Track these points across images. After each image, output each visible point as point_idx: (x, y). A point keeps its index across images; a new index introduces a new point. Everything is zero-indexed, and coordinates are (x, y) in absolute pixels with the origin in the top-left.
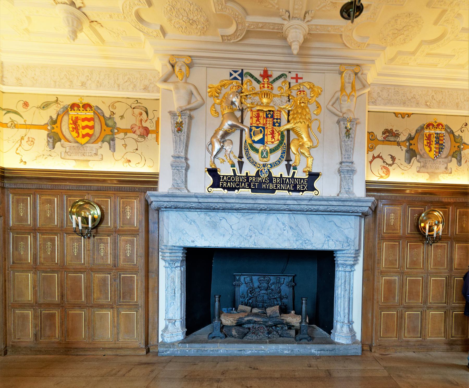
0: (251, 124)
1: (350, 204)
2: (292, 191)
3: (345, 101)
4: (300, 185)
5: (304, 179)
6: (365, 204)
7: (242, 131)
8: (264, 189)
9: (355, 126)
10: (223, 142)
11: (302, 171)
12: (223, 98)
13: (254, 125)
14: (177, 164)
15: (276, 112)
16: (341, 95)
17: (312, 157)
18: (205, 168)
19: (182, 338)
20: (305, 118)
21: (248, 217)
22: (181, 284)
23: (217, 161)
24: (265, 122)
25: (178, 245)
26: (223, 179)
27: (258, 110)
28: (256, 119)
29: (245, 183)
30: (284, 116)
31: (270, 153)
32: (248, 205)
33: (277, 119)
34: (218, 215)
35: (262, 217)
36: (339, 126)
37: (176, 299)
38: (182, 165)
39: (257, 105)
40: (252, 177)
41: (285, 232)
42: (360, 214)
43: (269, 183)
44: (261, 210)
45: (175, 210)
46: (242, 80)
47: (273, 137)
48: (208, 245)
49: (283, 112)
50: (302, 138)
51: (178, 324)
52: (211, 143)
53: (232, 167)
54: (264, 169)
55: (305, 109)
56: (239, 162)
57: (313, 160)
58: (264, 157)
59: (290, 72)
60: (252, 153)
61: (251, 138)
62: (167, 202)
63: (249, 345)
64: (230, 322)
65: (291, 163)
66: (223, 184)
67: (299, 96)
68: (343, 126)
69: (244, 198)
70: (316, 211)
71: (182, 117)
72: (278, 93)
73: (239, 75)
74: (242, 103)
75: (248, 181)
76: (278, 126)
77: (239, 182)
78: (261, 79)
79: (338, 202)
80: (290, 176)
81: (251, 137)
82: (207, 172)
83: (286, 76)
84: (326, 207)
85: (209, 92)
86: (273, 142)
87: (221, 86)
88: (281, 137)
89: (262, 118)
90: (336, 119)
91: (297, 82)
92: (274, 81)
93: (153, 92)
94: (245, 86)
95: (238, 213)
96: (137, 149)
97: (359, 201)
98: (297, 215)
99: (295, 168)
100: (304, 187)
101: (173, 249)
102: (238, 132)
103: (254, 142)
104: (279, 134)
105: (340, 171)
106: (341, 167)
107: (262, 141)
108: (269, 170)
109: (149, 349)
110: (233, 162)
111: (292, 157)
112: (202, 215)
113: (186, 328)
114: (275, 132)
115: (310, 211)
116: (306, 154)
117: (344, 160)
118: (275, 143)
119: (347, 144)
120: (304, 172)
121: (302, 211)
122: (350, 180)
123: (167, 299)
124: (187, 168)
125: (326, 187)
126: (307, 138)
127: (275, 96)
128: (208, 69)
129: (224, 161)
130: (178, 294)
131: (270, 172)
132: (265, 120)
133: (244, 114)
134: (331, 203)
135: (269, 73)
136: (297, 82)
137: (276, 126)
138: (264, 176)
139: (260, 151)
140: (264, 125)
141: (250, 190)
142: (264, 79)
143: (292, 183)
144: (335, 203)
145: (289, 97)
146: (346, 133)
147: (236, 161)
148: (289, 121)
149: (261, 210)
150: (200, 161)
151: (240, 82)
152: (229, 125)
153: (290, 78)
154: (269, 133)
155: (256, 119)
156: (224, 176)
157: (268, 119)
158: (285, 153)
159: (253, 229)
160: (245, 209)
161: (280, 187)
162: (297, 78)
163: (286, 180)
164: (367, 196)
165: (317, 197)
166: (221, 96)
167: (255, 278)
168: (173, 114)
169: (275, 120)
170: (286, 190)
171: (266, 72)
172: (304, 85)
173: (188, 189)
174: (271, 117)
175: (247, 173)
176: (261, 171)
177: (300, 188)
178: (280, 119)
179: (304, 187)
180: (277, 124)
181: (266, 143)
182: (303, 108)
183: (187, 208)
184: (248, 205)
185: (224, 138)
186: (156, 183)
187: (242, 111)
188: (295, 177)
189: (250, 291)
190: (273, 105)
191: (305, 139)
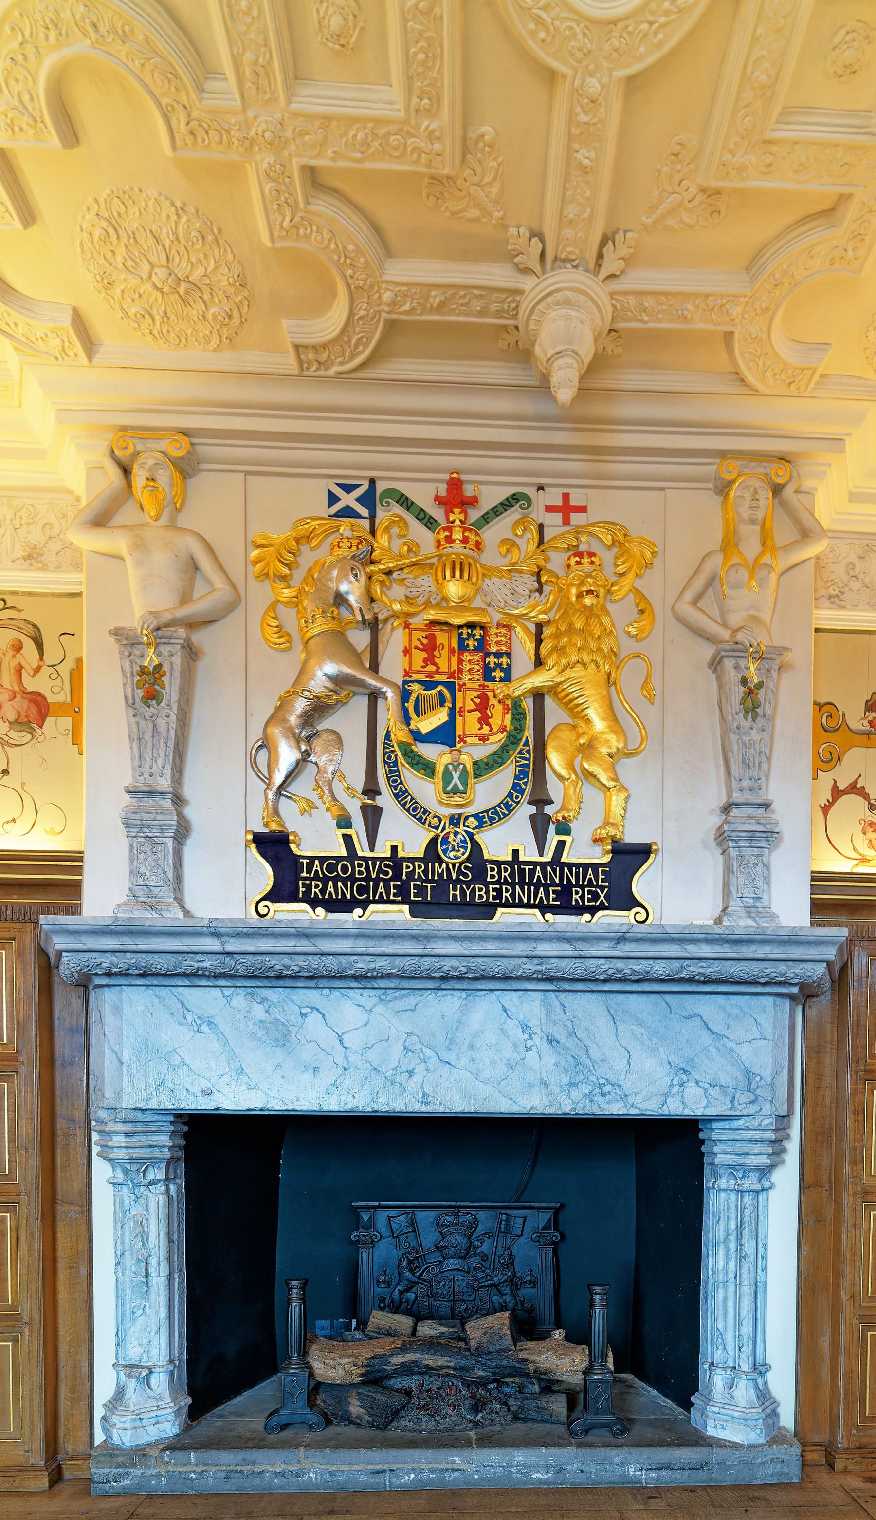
0: (407, 674)
2: (555, 910)
3: (738, 586)
4: (583, 887)
5: (595, 867)
6: (812, 953)
7: (375, 697)
8: (455, 904)
9: (774, 674)
10: (309, 739)
12: (305, 581)
13: (415, 677)
14: (146, 816)
15: (493, 631)
16: (724, 564)
17: (623, 788)
18: (247, 832)
19: (176, 1430)
20: (599, 649)
21: (399, 1005)
22: (170, 1241)
23: (285, 805)
24: (454, 667)
25: (154, 1104)
27: (433, 623)
28: (424, 655)
29: (386, 883)
30: (523, 646)
31: (476, 776)
32: (399, 962)
33: (498, 655)
34: (295, 998)
35: (450, 1003)
36: (719, 678)
37: (153, 1296)
38: (162, 821)
39: (428, 604)
40: (412, 860)
41: (531, 1056)
44: (445, 979)
45: (141, 982)
47: (484, 720)
48: (259, 1106)
49: (518, 629)
50: (588, 721)
51: (160, 1381)
52: (266, 744)
53: (339, 826)
55: (598, 616)
56: (364, 808)
57: (627, 799)
58: (455, 791)
59: (541, 488)
60: (411, 778)
61: (408, 724)
62: (114, 952)
63: (411, 1451)
64: (340, 1371)
67: (577, 572)
68: (732, 676)
69: (386, 937)
70: (638, 981)
71: (162, 648)
72: (502, 563)
74: (372, 600)
75: (397, 876)
76: (502, 680)
79: (717, 948)
80: (548, 857)
81: (407, 720)
82: (253, 847)
84: (676, 965)
86: (484, 739)
87: (297, 541)
88: (513, 718)
89: (445, 653)
90: (708, 652)
91: (566, 522)
92: (486, 519)
93: (58, 568)
94: (383, 540)
95: (366, 992)
96: (6, 772)
98: (571, 996)
100: (595, 896)
101: (137, 1120)
102: (361, 704)
103: (417, 736)
104: (506, 710)
105: (722, 838)
106: (726, 822)
107: (445, 735)
108: (471, 836)
109: (59, 1467)
110: (342, 808)
112: (239, 999)
113: (190, 1394)
114: (492, 701)
115: (620, 980)
116: (603, 778)
117: (737, 797)
118: (492, 739)
119: (746, 739)
121: (589, 982)
122: (759, 868)
123: (119, 1295)
124: (182, 832)
125: (676, 895)
126: (603, 719)
127: (489, 572)
128: (249, 477)
129: (312, 806)
130: (159, 1280)
131: (475, 844)
132: (454, 660)
133: (382, 639)
134: (693, 950)
136: (566, 522)
137: (493, 679)
138: (455, 856)
139: (440, 769)
140: (452, 675)
141: (406, 908)
142: (449, 512)
143: (553, 883)
144: (706, 950)
145: (538, 575)
148: (539, 662)
149: (445, 979)
150: (225, 805)
151: (366, 524)
152: (328, 676)
153: (542, 509)
154: (470, 705)
155: (424, 655)
157: (467, 657)
158: (526, 774)
159: (419, 1046)
160: (389, 976)
161: (513, 895)
162: (566, 509)
163: (532, 872)
164: (812, 924)
165: (642, 928)
166: (299, 575)
167: (425, 1218)
168: (127, 639)
169: (492, 660)
170: (533, 906)
172: (590, 534)
173: (188, 906)
174: (477, 649)
175: (394, 849)
177: (582, 897)
179: (595, 896)
180: (498, 674)
181: (462, 740)
182: (589, 612)
183: (184, 975)
184: (398, 961)
185: (312, 725)
186: (75, 888)
187: (374, 626)
189: (410, 1262)
190: (484, 606)
191: (599, 724)
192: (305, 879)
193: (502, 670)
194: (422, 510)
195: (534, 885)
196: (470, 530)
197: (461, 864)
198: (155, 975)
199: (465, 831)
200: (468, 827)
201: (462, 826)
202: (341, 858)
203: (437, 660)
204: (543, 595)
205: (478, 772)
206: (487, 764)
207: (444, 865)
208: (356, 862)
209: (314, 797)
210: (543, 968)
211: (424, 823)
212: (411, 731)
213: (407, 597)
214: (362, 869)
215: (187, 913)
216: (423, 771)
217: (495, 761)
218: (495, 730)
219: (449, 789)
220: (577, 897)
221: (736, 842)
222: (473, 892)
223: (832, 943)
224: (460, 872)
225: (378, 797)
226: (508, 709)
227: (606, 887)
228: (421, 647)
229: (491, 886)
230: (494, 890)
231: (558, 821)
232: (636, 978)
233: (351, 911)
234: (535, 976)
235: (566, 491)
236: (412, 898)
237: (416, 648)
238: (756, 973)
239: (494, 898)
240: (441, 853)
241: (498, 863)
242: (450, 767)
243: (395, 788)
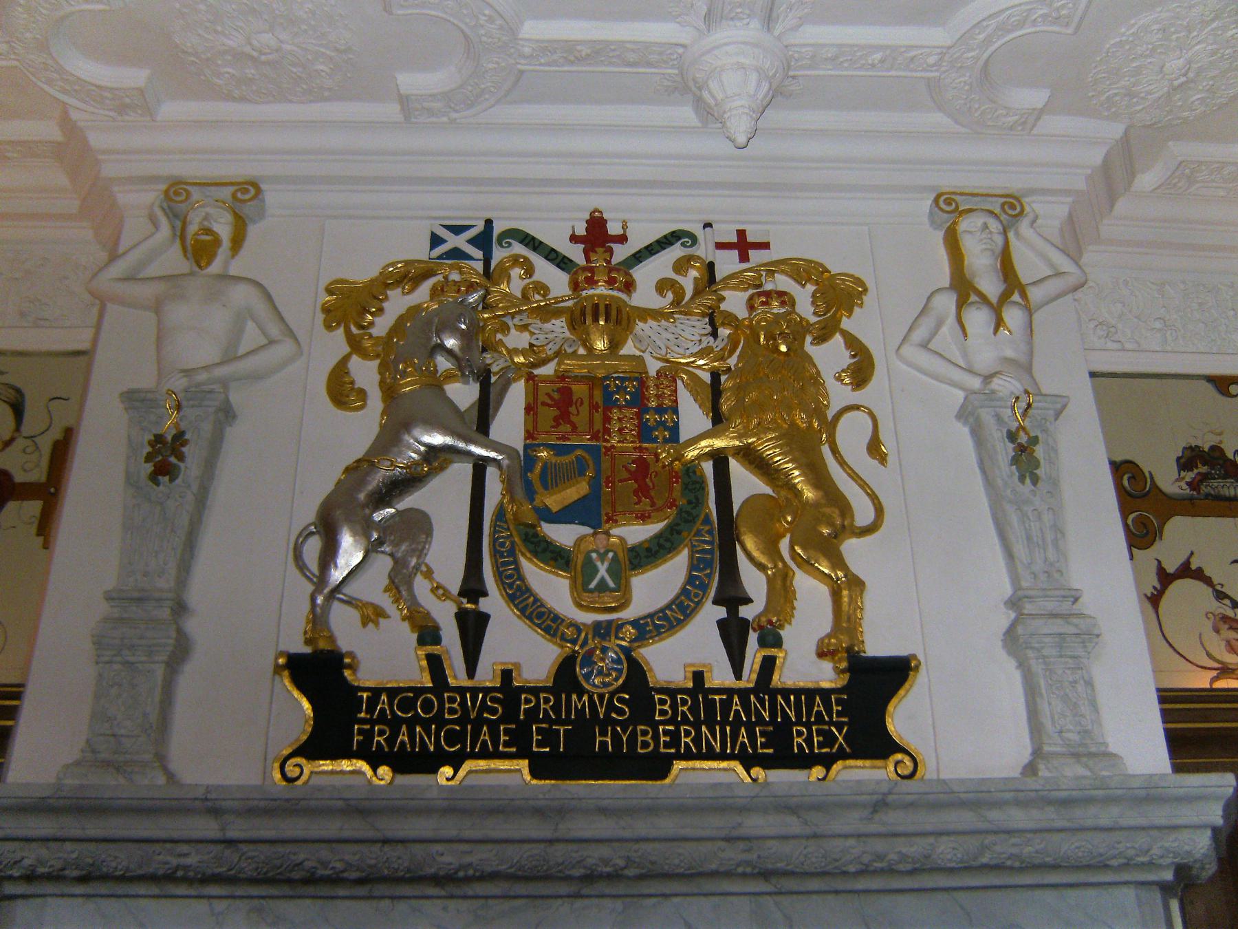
0: (529, 435)
1: (1107, 816)
2: (768, 763)
4: (808, 725)
5: (825, 694)
6: (1187, 815)
11: (812, 647)
24: (598, 425)
26: (370, 710)
28: (553, 412)
33: (660, 410)
40: (535, 691)
42: (1168, 876)
43: (634, 720)
46: (487, 261)
54: (604, 650)
56: (461, 616)
59: (708, 225)
60: (536, 575)
61: (532, 500)
62: (45, 840)
65: (746, 612)
66: (368, 735)
70: (912, 872)
73: (471, 241)
77: (463, 721)
78: (576, 253)
79: (1035, 813)
80: (749, 679)
81: (530, 493)
82: (286, 673)
83: (694, 239)
84: (972, 843)
85: (327, 310)
89: (585, 409)
91: (744, 258)
92: (638, 258)
97: (1148, 795)
99: (771, 639)
111: (754, 581)
115: (882, 871)
120: (821, 655)
132: (598, 417)
135: (614, 229)
137: (655, 440)
138: (602, 680)
140: (595, 437)
141: (524, 764)
146: (1015, 461)
147: (445, 615)
149: (590, 878)
151: (479, 266)
153: (711, 246)
155: (553, 412)
156: (376, 692)
158: (709, 564)
160: (494, 876)
161: (697, 741)
162: (743, 245)
163: (726, 705)
171: (597, 224)
174: (629, 405)
176: (588, 659)
177: (809, 741)
178: (676, 411)
179: (829, 739)
183: (153, 878)
184: (510, 850)
188: (777, 680)
192: (363, 721)
193: (666, 428)
194: (553, 250)
195: (730, 724)
196: (618, 270)
197: (612, 694)
198: (105, 878)
199: (620, 646)
200: (623, 639)
201: (613, 638)
202: (424, 690)
203: (574, 419)
204: (719, 339)
205: (636, 562)
206: (648, 550)
207: (585, 698)
208: (446, 695)
209: (385, 601)
210: (753, 856)
211: (554, 636)
212: (536, 509)
213: (531, 345)
214: (455, 706)
215: (171, 777)
216: (552, 562)
217: (660, 546)
218: (659, 503)
219: (592, 586)
220: (800, 740)
221: (1038, 650)
222: (633, 738)
223: (1218, 798)
224: (611, 707)
225: (482, 600)
226: (677, 477)
227: (843, 723)
228: (549, 401)
229: (661, 728)
230: (666, 733)
231: (761, 627)
232: (909, 867)
233: (435, 771)
234: (740, 870)
235: (741, 227)
236: (535, 749)
237: (544, 404)
238: (1101, 851)
239: (666, 745)
240: (580, 678)
241: (672, 692)
242: (594, 555)
243: (511, 586)
